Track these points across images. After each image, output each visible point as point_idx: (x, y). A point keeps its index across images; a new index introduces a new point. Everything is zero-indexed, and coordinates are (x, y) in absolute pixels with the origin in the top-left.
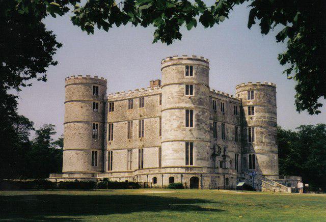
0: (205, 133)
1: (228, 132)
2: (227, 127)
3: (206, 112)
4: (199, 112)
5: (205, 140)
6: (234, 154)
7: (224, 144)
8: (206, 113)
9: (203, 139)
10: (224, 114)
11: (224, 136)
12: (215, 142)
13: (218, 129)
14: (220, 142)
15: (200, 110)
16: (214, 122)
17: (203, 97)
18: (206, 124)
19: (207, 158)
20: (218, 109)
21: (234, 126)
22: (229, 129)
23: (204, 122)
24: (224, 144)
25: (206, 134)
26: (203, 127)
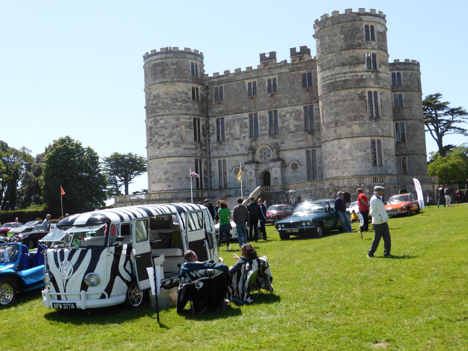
0: (158, 148)
1: (283, 122)
2: (283, 113)
3: (161, 120)
4: (151, 123)
5: (158, 156)
6: (303, 152)
7: (275, 141)
8: (161, 121)
9: (157, 156)
10: (272, 96)
11: (274, 130)
12: (254, 144)
13: (259, 122)
14: (265, 141)
15: (152, 119)
16: (251, 116)
17: (155, 102)
18: (160, 136)
19: (163, 180)
20: (262, 93)
21: (301, 108)
22: (288, 115)
23: (158, 134)
24: (275, 141)
25: (162, 147)
26: (156, 141)
